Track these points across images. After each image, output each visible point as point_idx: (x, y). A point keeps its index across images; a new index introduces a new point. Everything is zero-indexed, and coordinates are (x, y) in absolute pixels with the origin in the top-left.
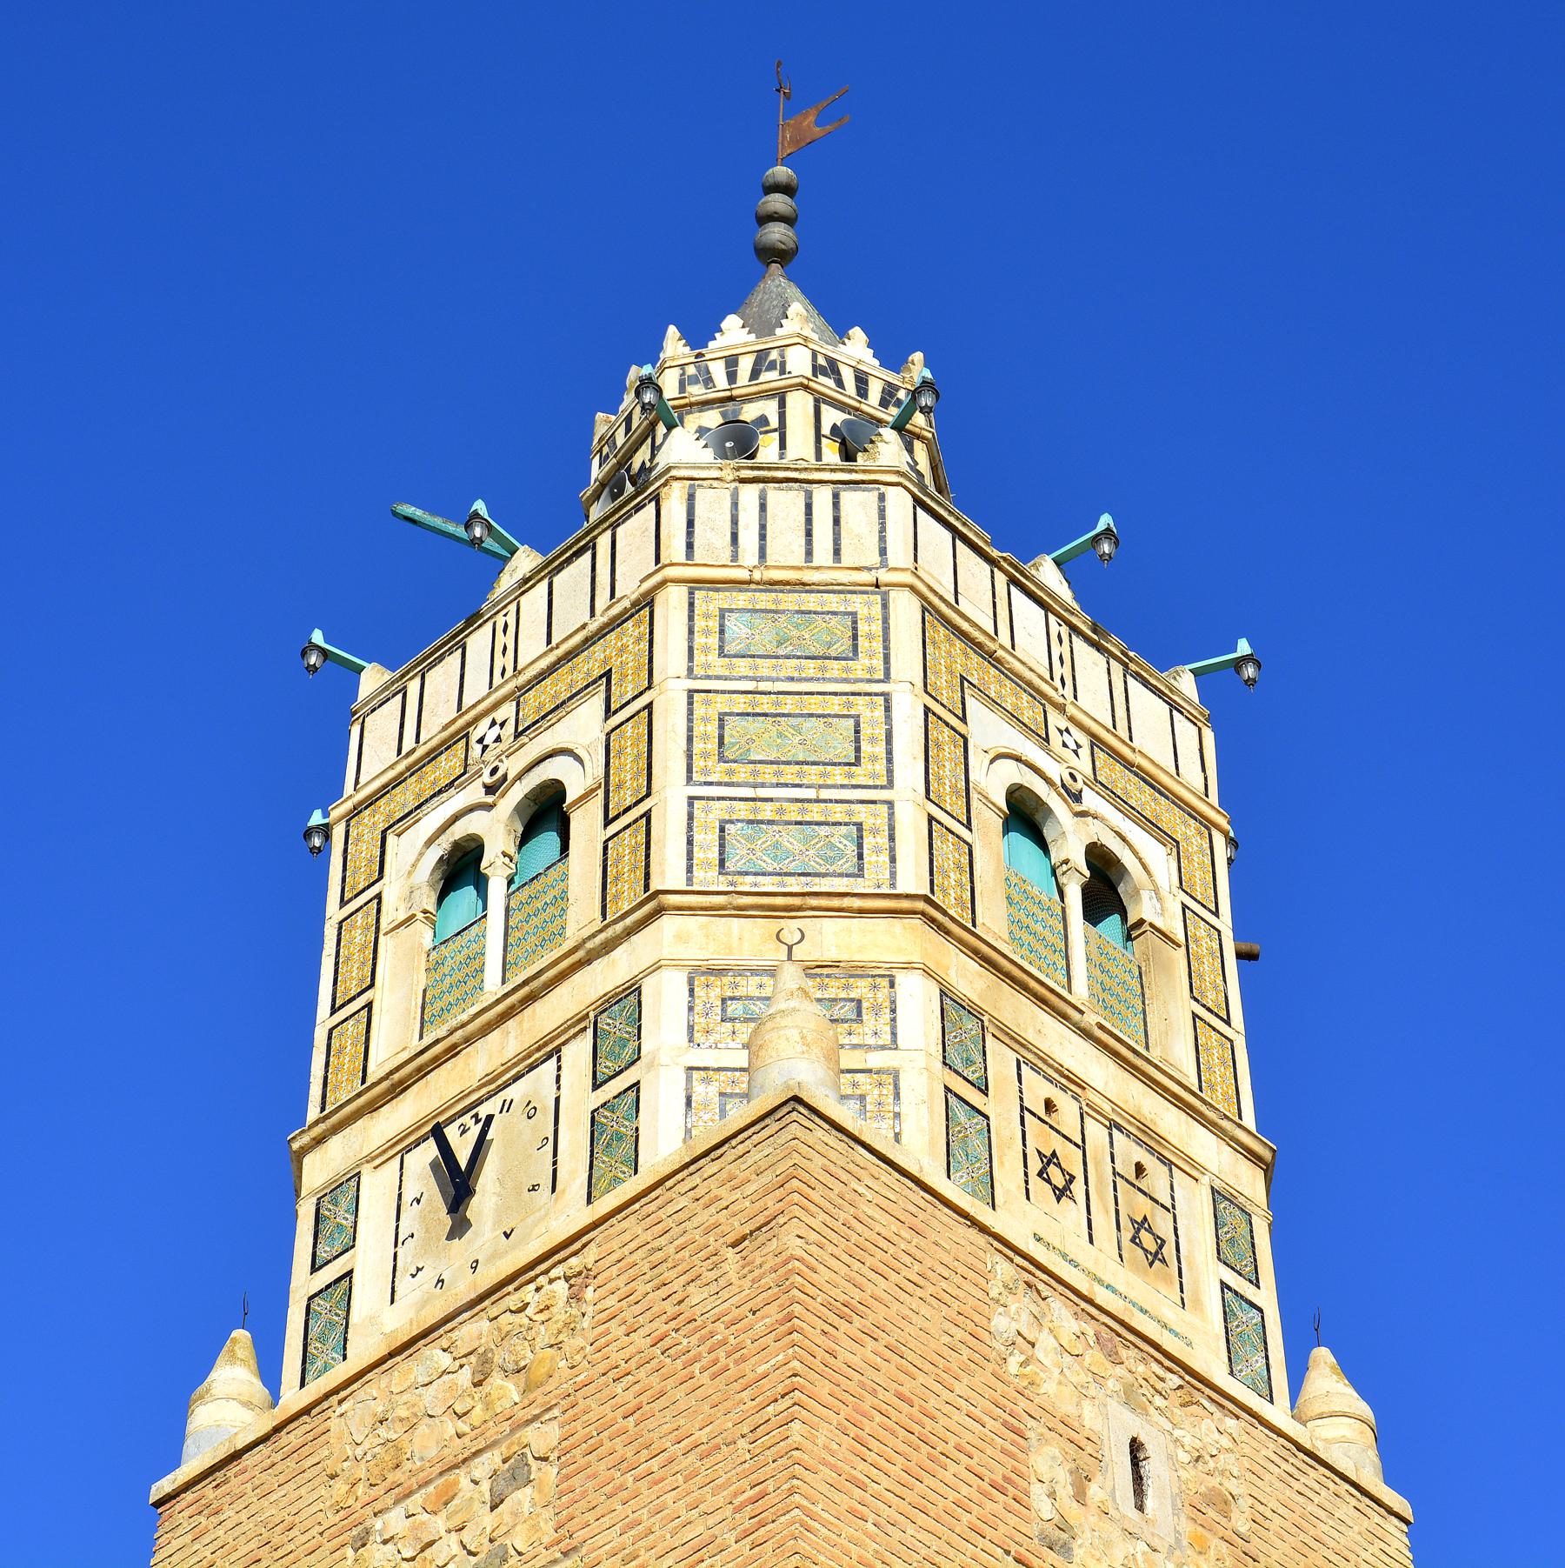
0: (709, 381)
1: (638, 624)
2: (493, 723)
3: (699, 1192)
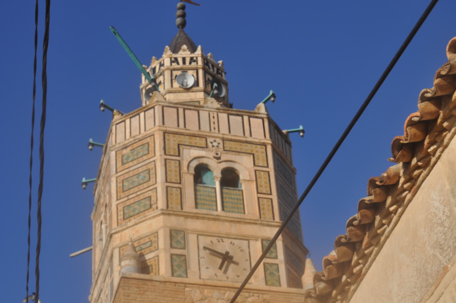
0: (209, 68)
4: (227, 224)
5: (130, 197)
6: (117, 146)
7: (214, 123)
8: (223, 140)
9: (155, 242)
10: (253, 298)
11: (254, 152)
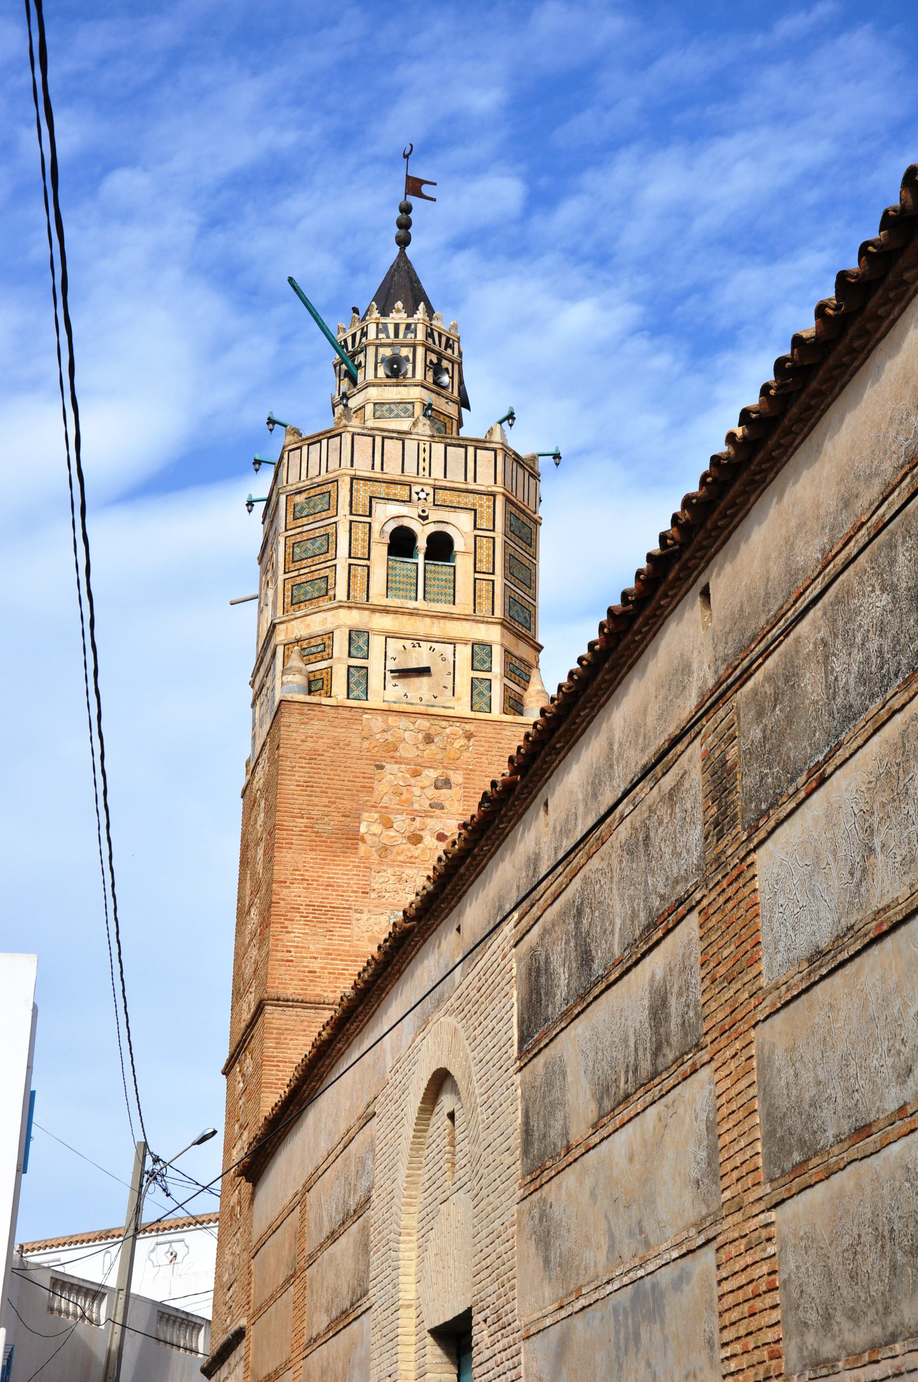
0: (434, 343)
2: (422, 490)
4: (427, 620)
5: (302, 571)
6: (289, 488)
7: (424, 460)
8: (435, 488)
9: (329, 646)
11: (477, 507)
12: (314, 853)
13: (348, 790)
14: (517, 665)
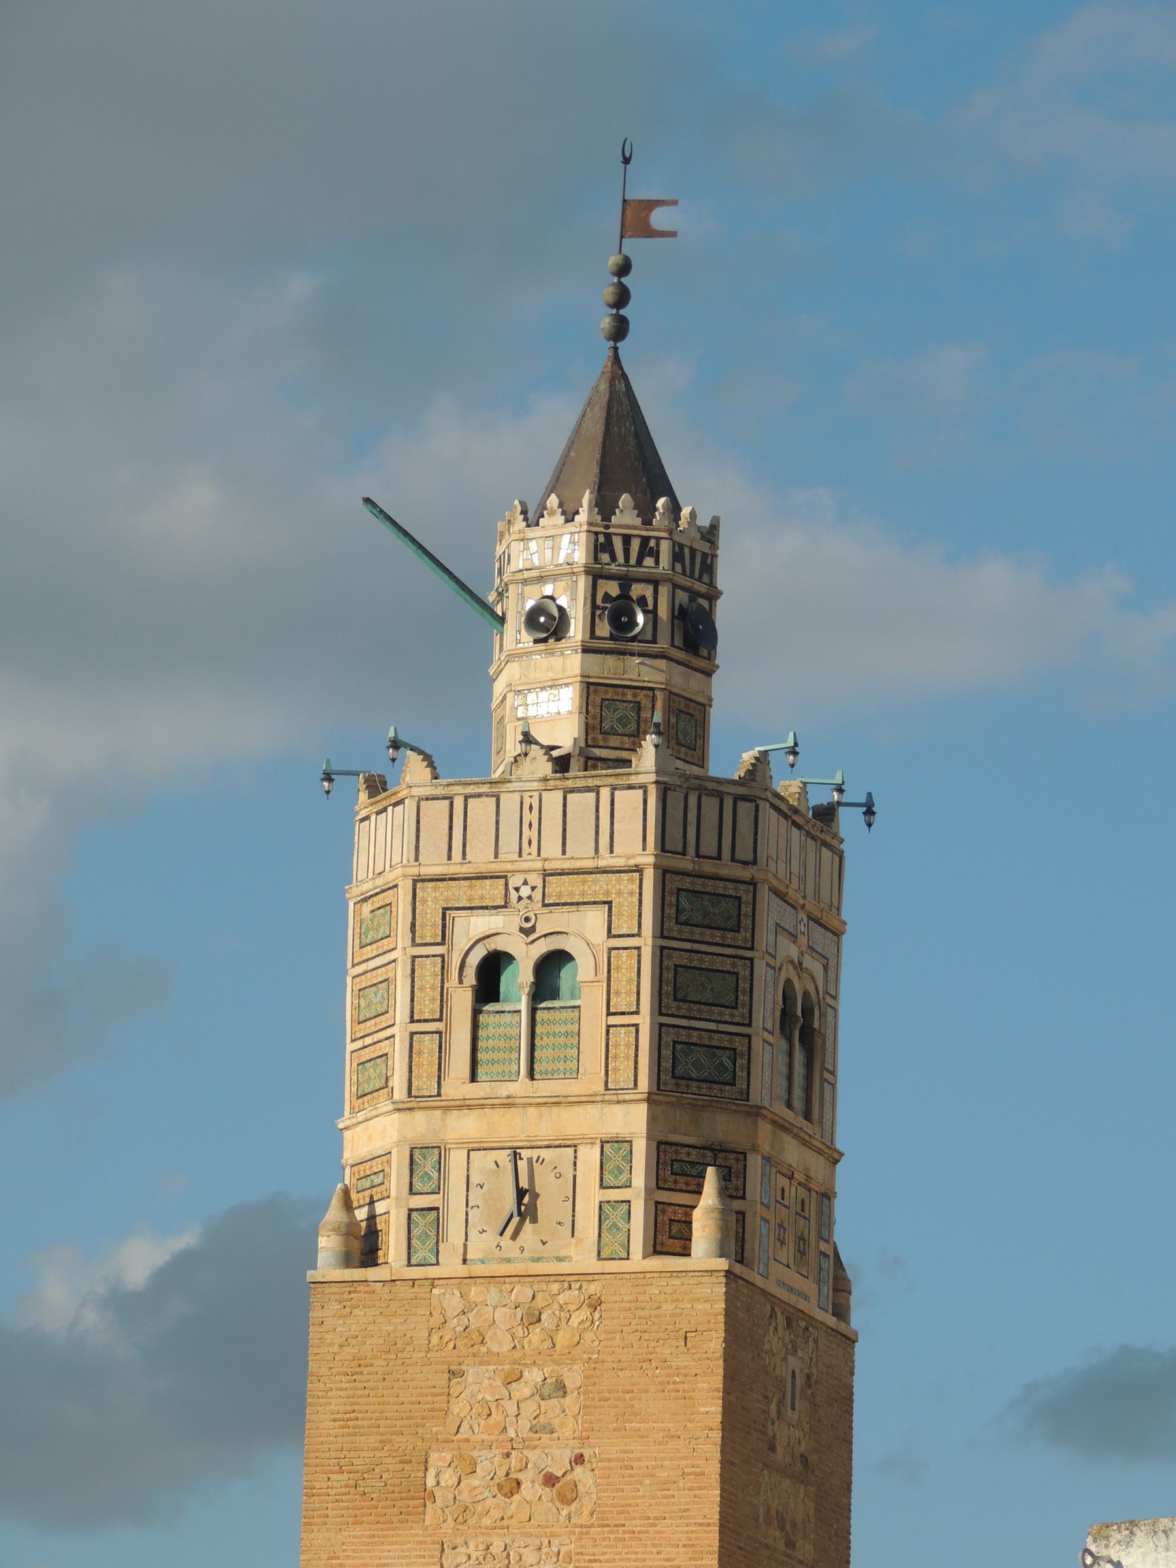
0: (613, 558)
1: (631, 880)
2: (525, 883)
3: (669, 1290)
4: (532, 1111)
8: (546, 874)
10: (567, 1293)
11: (612, 897)
12: (358, 1527)
13: (408, 1418)
14: (693, 1158)
